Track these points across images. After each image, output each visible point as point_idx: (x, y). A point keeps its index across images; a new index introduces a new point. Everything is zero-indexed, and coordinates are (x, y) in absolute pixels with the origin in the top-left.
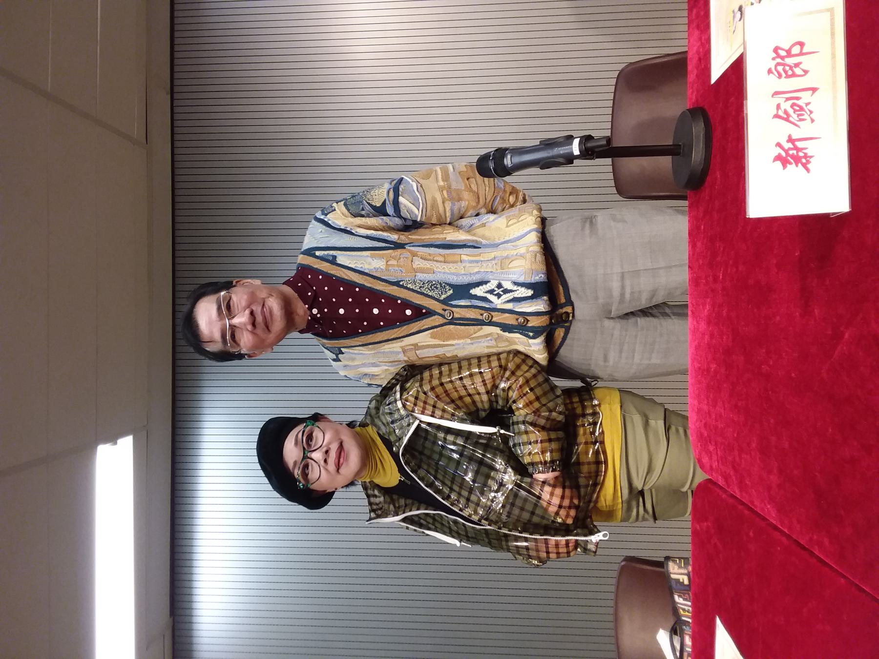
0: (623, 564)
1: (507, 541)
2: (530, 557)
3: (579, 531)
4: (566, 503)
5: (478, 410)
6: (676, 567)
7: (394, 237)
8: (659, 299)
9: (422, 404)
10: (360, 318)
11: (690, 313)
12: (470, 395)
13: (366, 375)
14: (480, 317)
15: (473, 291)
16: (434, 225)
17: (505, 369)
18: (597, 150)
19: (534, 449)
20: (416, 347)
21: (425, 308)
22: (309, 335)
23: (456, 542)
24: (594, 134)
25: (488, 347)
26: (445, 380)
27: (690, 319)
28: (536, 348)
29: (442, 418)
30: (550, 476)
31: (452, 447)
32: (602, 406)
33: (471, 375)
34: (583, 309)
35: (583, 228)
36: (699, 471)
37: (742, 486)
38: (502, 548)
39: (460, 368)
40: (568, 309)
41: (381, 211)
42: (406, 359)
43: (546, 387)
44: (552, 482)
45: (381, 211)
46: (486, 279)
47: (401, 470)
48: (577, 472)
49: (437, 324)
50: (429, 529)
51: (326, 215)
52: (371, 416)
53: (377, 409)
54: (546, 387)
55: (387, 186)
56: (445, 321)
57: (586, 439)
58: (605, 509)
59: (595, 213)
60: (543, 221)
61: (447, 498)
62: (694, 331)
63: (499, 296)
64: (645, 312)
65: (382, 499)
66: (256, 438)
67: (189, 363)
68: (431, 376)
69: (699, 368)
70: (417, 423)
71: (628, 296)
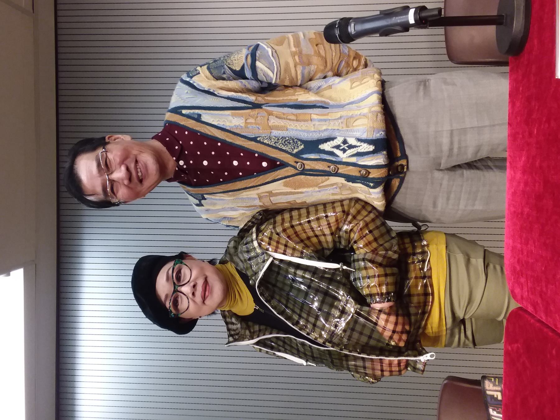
0: (445, 382)
1: (347, 361)
2: (366, 374)
3: (410, 352)
4: (399, 328)
5: (323, 249)
6: (491, 385)
7: (252, 98)
8: (483, 154)
9: (275, 244)
10: (222, 169)
11: (508, 164)
12: (316, 236)
13: (225, 218)
14: (328, 169)
15: (322, 147)
16: (286, 87)
17: (348, 214)
18: (430, 19)
19: (372, 282)
20: (271, 194)
21: (280, 160)
22: (175, 184)
23: (304, 363)
24: (429, 6)
25: (333, 194)
26: (295, 223)
27: (508, 170)
28: (375, 197)
29: (292, 255)
30: (385, 305)
31: (300, 280)
32: (431, 247)
33: (318, 219)
34: (416, 161)
35: (418, 90)
36: (513, 302)
37: (547, 312)
38: (343, 367)
39: (308, 213)
40: (403, 162)
41: (240, 75)
42: (261, 204)
43: (383, 229)
44: (387, 311)
45: (240, 75)
46: (333, 136)
47: (257, 300)
48: (408, 303)
49: (290, 174)
50: (279, 351)
51: (191, 77)
52: (230, 254)
53: (236, 248)
54: (383, 229)
55: (245, 52)
56: (297, 171)
57: (416, 274)
58: (431, 335)
59: (428, 77)
60: (383, 84)
61: (297, 323)
62: (512, 180)
63: (344, 151)
64: (470, 165)
65: (239, 326)
66: (131, 273)
67: (69, 212)
68: (283, 220)
69: (515, 212)
70: (271, 259)
71: (455, 150)
